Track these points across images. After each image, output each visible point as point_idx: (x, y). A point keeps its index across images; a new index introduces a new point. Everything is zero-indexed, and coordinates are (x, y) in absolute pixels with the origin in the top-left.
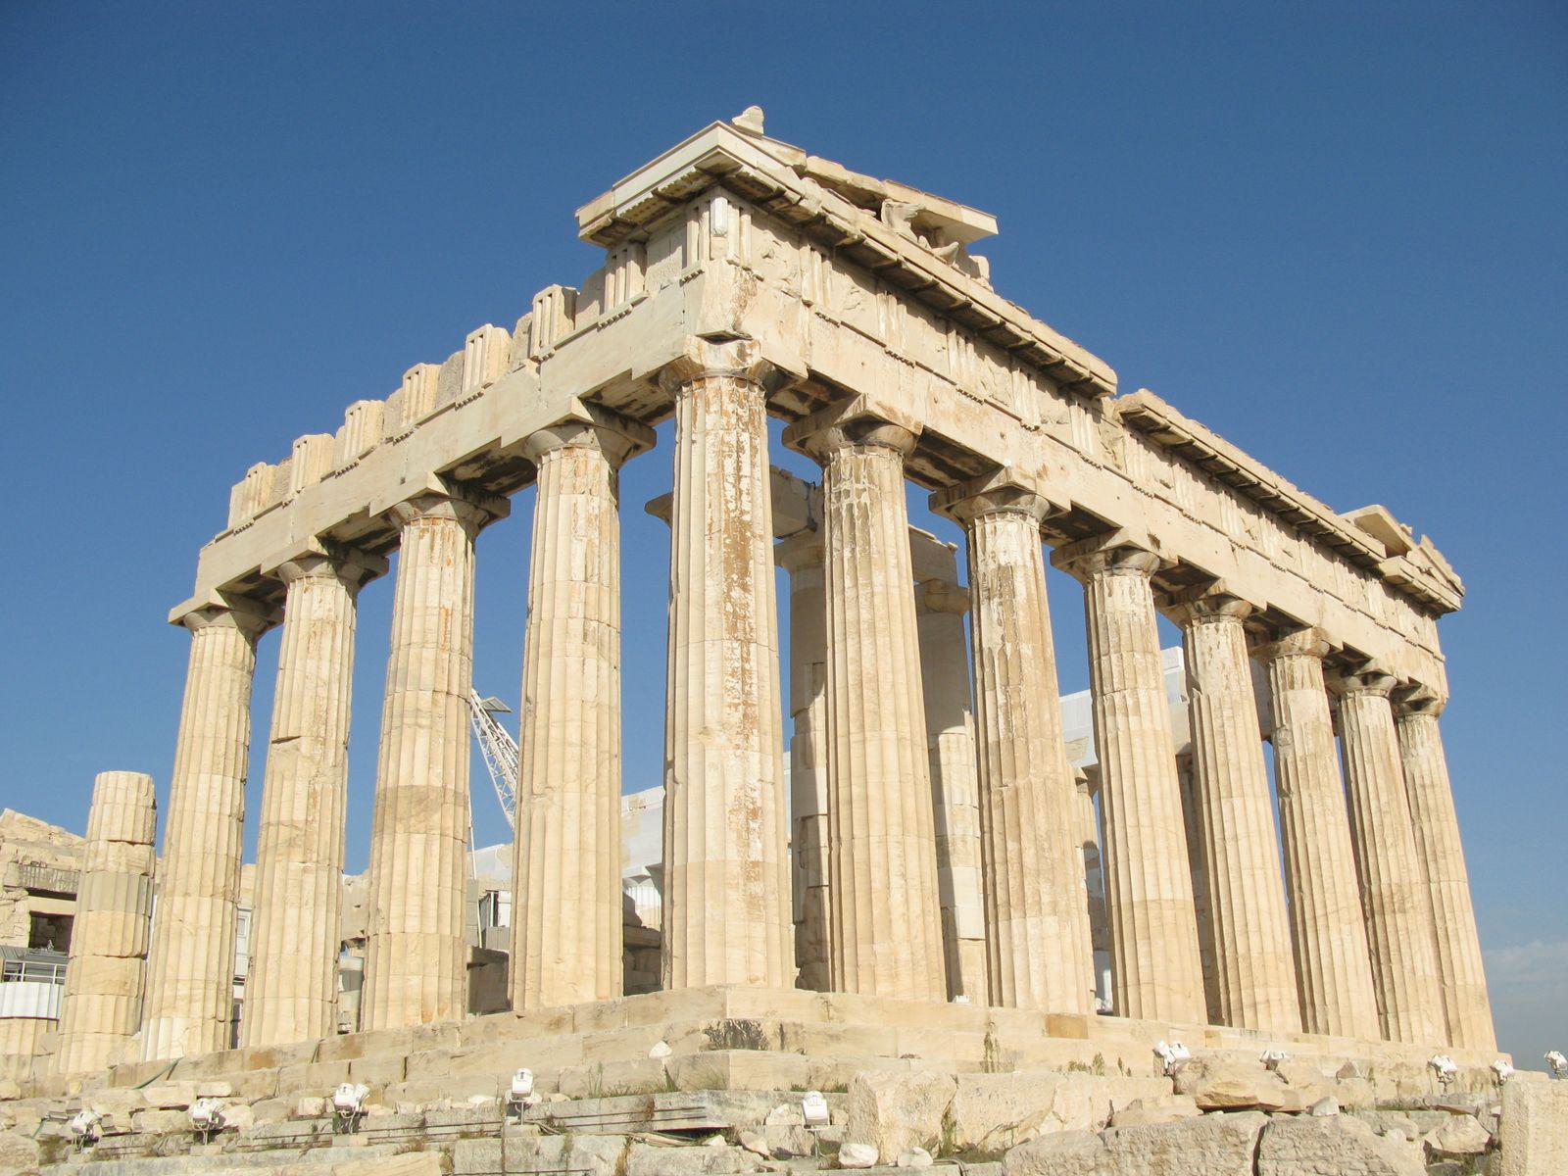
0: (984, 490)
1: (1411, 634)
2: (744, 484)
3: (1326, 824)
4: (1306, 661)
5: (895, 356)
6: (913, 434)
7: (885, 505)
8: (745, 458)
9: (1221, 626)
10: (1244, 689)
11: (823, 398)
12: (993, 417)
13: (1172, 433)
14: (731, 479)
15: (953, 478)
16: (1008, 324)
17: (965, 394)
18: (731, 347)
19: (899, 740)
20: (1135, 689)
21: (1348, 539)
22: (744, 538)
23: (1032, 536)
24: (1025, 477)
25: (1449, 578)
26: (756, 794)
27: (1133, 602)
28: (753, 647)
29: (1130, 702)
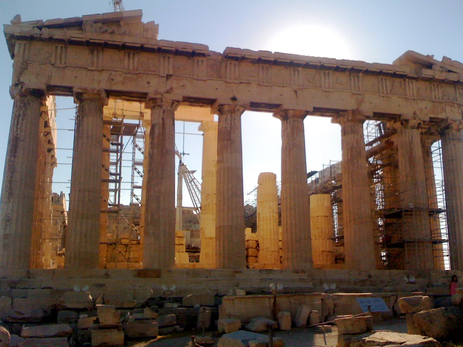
2: (19, 127)
3: (353, 186)
4: (350, 124)
7: (85, 119)
8: (20, 118)
9: (289, 121)
13: (247, 58)
14: (16, 126)
16: (145, 46)
18: (20, 87)
19: (79, 191)
20: (223, 154)
22: (17, 142)
24: (156, 94)
26: (10, 215)
28: (15, 173)
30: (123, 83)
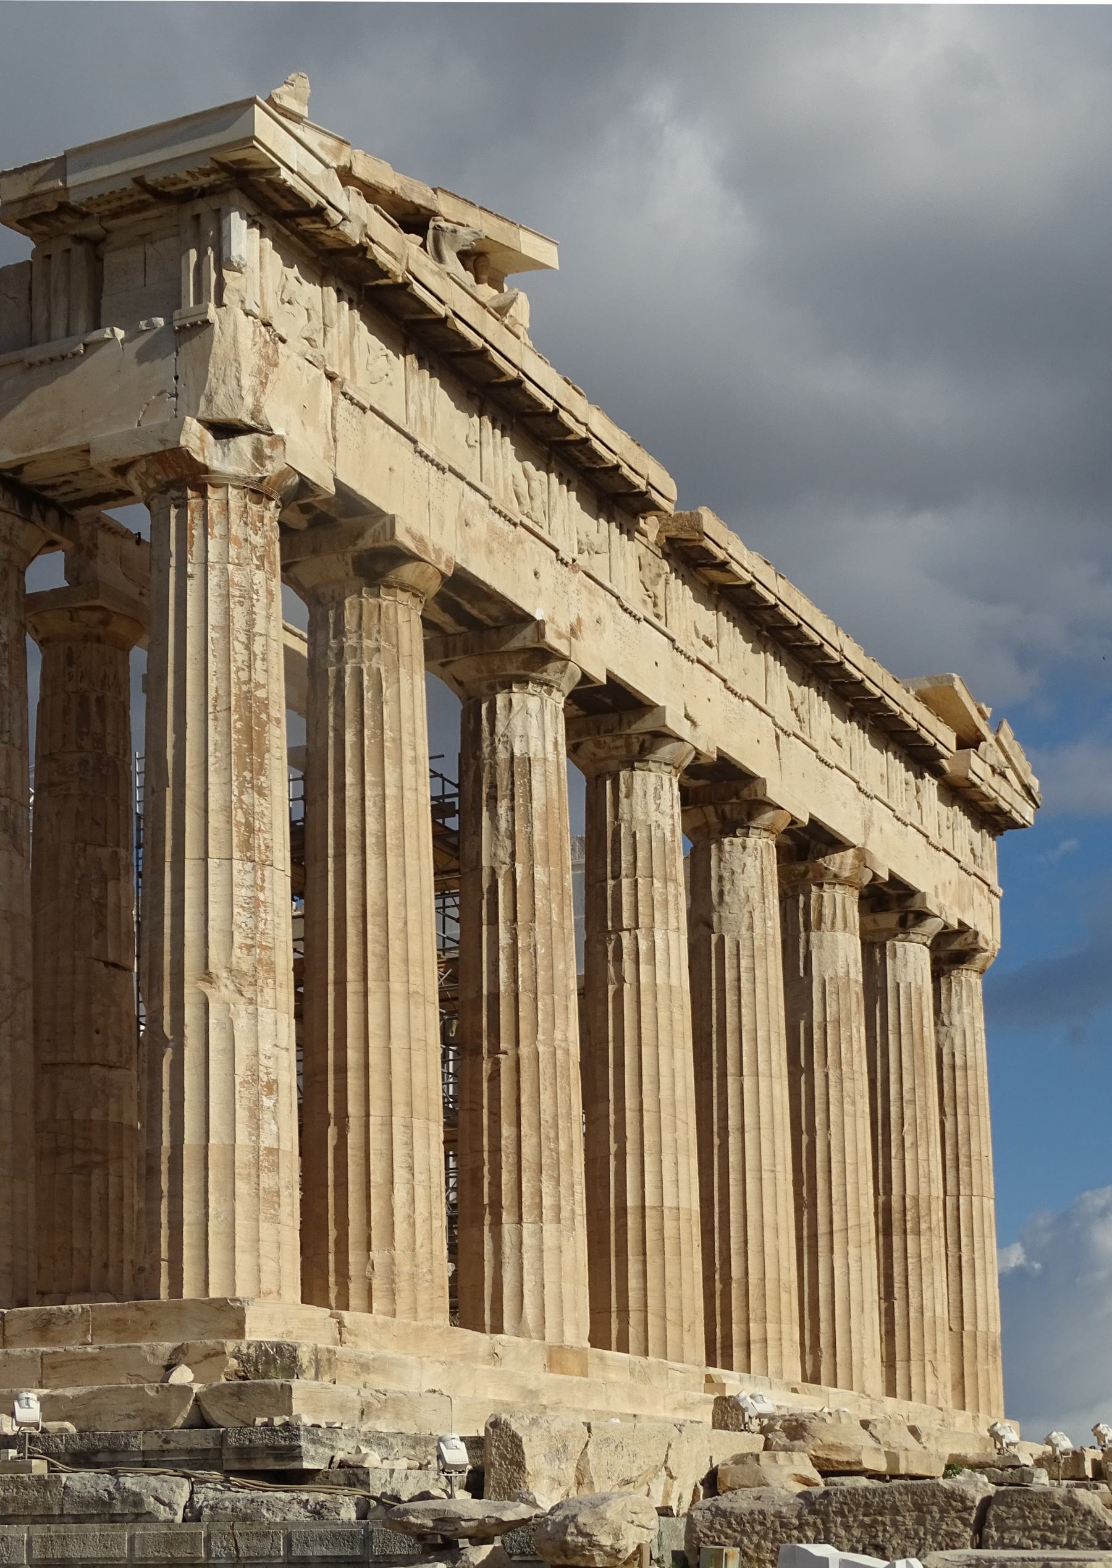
0: (502, 649)
1: (966, 859)
5: (426, 457)
6: (443, 575)
9: (750, 842)
10: (770, 931)
11: (332, 513)
12: (526, 546)
15: (459, 622)
17: (500, 513)
19: (408, 995)
20: (651, 928)
21: (914, 725)
23: (557, 717)
25: (1026, 781)
27: (657, 809)
29: (643, 945)
30: (490, 552)
